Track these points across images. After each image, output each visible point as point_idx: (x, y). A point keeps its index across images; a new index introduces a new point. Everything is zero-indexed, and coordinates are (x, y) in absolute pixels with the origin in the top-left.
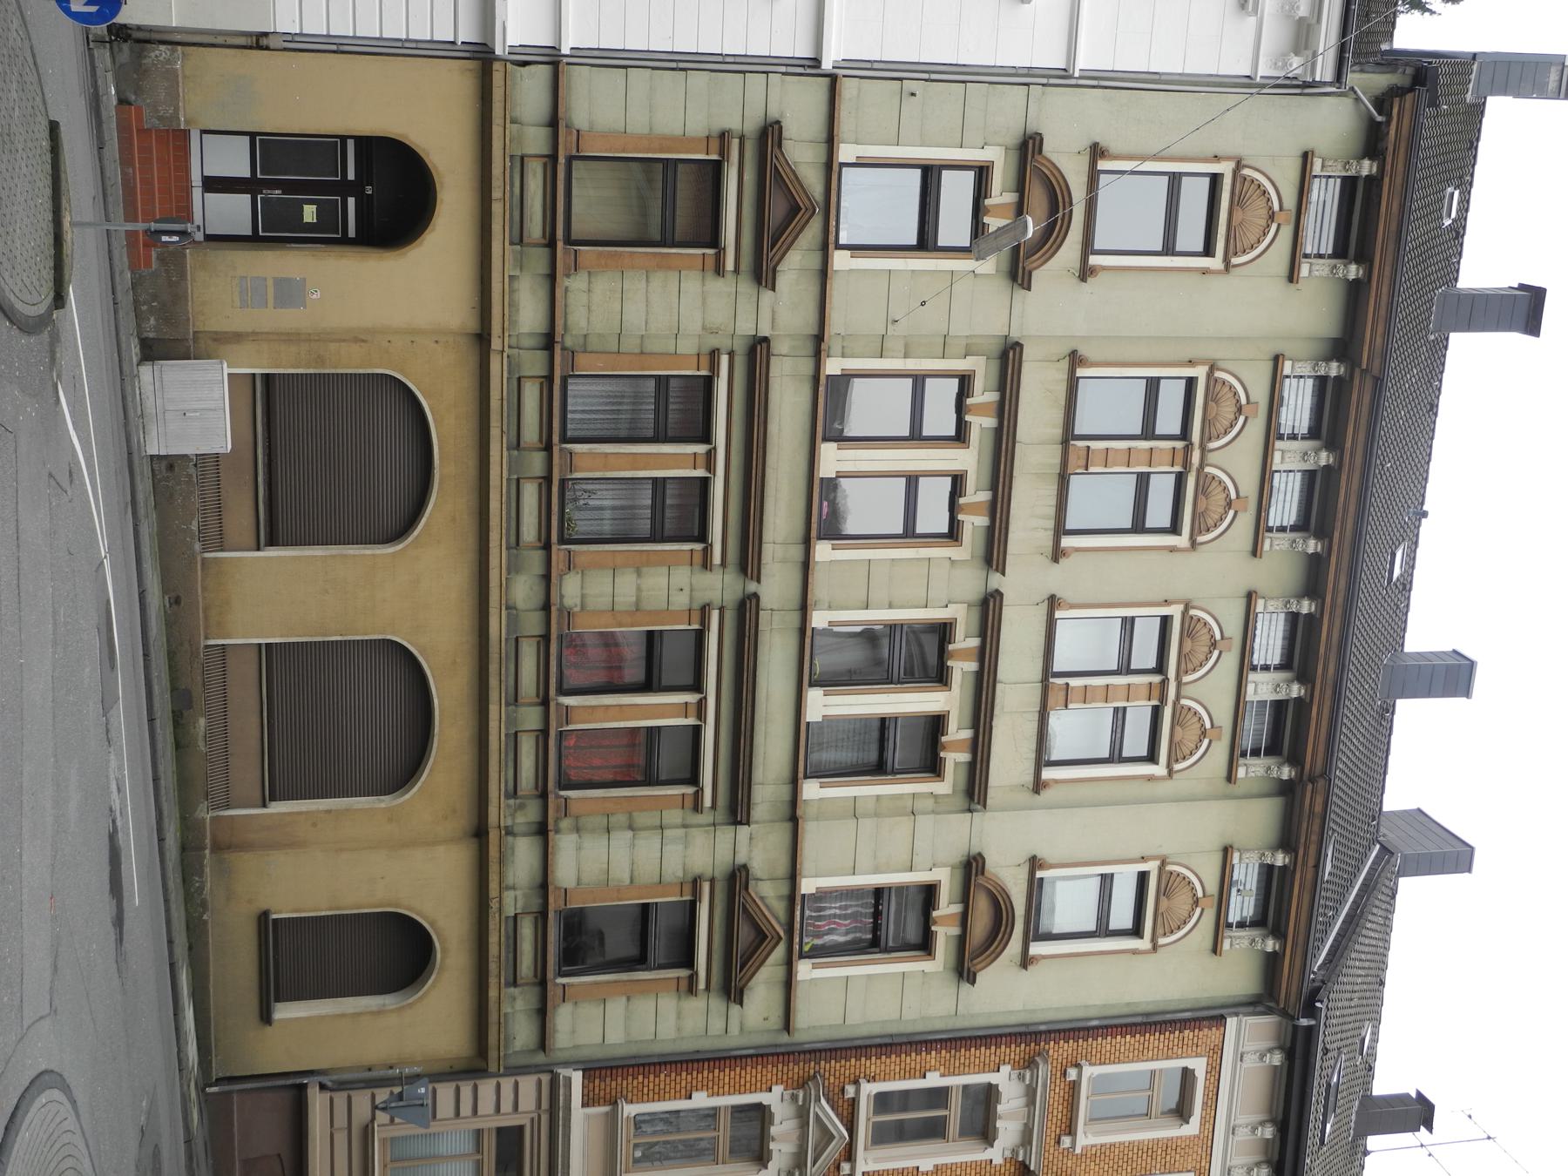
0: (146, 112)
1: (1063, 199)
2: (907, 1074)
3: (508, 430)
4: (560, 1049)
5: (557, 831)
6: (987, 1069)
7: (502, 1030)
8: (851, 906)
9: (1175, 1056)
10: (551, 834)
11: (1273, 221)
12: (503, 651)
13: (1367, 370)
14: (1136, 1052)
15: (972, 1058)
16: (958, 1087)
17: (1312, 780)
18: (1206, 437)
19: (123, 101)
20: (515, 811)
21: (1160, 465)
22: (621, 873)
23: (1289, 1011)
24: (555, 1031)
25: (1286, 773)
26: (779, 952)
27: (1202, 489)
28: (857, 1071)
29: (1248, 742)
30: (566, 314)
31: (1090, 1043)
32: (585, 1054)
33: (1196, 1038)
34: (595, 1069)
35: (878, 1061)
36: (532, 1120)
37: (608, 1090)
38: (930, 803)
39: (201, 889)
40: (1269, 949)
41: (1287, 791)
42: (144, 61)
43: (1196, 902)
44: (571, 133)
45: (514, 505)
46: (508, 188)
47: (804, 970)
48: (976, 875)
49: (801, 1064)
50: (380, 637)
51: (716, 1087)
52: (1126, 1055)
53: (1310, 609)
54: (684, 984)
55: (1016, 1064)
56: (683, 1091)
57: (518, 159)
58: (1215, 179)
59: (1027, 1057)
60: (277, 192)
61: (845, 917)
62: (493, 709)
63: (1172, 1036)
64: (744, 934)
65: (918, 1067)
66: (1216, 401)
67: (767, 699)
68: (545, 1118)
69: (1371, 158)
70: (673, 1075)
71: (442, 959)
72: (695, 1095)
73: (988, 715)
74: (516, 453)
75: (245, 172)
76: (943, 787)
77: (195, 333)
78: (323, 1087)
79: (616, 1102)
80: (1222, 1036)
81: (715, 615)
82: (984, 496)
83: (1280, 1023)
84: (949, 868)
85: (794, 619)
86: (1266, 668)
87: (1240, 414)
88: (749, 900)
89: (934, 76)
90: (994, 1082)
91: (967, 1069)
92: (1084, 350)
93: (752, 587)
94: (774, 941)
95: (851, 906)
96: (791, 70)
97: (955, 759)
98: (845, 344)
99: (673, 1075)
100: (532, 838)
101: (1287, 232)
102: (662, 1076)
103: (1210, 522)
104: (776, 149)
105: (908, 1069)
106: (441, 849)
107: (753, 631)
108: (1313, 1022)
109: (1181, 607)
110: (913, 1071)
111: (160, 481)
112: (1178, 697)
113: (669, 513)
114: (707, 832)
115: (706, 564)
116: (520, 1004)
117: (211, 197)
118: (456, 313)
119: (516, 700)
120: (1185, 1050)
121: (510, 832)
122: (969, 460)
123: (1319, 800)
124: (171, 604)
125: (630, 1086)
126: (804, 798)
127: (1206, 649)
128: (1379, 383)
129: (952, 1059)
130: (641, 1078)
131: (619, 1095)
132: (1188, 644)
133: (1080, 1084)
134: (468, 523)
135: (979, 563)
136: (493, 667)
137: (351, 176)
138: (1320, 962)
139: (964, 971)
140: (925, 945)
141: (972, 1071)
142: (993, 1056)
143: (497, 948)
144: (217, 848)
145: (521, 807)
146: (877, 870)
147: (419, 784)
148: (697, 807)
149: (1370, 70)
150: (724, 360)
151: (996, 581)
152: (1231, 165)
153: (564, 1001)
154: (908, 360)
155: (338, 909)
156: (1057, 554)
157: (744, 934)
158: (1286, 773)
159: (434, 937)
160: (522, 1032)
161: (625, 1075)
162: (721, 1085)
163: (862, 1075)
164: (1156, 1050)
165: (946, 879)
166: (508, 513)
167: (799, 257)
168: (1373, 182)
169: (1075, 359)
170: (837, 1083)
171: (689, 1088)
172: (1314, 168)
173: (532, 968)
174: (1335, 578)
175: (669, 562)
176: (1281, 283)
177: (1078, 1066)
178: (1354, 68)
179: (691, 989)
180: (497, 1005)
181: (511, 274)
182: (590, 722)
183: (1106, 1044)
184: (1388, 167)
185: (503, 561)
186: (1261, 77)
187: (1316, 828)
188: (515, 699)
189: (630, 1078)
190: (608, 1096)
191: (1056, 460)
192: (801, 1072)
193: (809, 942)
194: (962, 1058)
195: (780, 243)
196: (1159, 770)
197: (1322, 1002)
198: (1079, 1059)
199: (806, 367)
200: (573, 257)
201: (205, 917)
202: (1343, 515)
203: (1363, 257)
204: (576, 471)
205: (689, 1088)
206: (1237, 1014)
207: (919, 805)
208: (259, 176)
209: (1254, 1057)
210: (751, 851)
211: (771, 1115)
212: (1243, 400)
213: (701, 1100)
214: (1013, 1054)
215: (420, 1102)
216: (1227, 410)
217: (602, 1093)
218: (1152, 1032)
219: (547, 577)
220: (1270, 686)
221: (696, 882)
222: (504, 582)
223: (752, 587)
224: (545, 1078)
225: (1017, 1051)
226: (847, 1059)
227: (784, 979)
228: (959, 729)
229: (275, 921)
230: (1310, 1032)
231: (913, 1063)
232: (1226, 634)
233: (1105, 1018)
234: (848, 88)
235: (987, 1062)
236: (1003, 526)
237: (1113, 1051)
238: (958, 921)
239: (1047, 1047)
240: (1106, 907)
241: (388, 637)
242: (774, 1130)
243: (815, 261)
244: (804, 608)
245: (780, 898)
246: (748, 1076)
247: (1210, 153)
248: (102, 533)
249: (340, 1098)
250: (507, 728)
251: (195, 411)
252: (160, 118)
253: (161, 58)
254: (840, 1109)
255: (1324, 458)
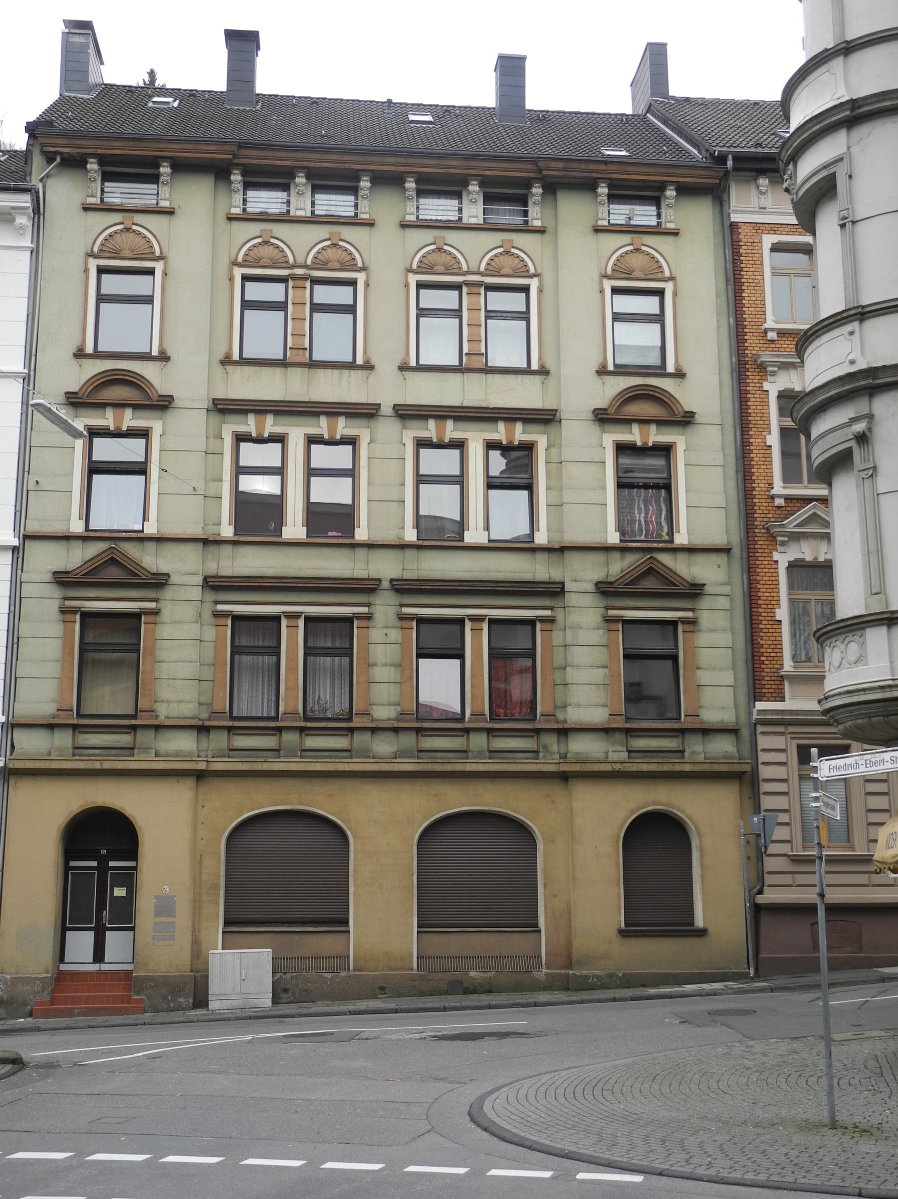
0: (39, 999)
1: (110, 376)
2: (768, 459)
3: (263, 757)
4: (737, 718)
5: (565, 721)
6: (766, 400)
7: (716, 761)
8: (639, 505)
9: (760, 259)
10: (566, 726)
11: (130, 229)
12: (425, 761)
13: (233, 154)
14: (756, 288)
15: (756, 411)
16: (780, 421)
17: (540, 171)
18: (286, 265)
19: (31, 1014)
20: (549, 752)
21: (304, 296)
22: (599, 675)
23: (722, 175)
24: (722, 722)
25: (537, 190)
26: (666, 559)
27: (323, 265)
28: (763, 497)
29: (518, 220)
30: (184, 718)
31: (748, 323)
32: (742, 699)
33: (747, 244)
34: (755, 692)
35: (756, 481)
36: (792, 738)
37: (772, 682)
38: (554, 451)
39: (598, 977)
40: (674, 193)
41: (551, 189)
42: (5, 999)
43: (637, 250)
44: (58, 715)
45: (321, 753)
46: (93, 758)
47: (681, 539)
48: (608, 414)
49: (756, 539)
50: (415, 848)
51: (773, 602)
52: (759, 295)
53: (476, 185)
54: (689, 627)
55: (763, 378)
56: (775, 626)
57: (76, 751)
58: (101, 271)
59: (757, 370)
60: (104, 914)
61: (647, 510)
62: (469, 768)
63: (744, 262)
64: (114, 573)
65: (763, 451)
66: (259, 260)
67: (471, 571)
68: (792, 729)
69: (86, 162)
70: (761, 634)
71: (661, 804)
72: (778, 618)
73: (485, 411)
74: (282, 752)
75: (91, 935)
76: (542, 442)
77: (191, 972)
78: (760, 892)
79: (782, 676)
80: (746, 224)
81: (406, 610)
82: (323, 421)
83: (737, 181)
84: (604, 435)
85: (410, 554)
86: (460, 210)
87: (269, 242)
88: (621, 581)
89: (26, 469)
90: (776, 394)
91: (765, 415)
92: (221, 355)
93: (386, 584)
94: (654, 562)
95: (639, 505)
96: (20, 566)
97: (520, 434)
98: (211, 523)
99: (761, 634)
100: (569, 740)
101: (139, 218)
102: (762, 642)
103: (348, 258)
104: (70, 575)
105: (764, 459)
106: (574, 805)
107: (416, 583)
108: (730, 157)
109: (410, 275)
110: (765, 455)
111: (295, 998)
112: (478, 273)
113: (338, 645)
114: (569, 614)
115: (368, 617)
116: (698, 748)
117: (107, 958)
118: (183, 791)
119: (465, 751)
120: (756, 252)
121: (564, 756)
122: (296, 434)
123: (554, 164)
124: (385, 994)
125: (769, 666)
126: (547, 543)
127: (443, 255)
128: (241, 145)
129: (757, 426)
130: (762, 658)
131: (776, 674)
132: (438, 268)
133: (780, 329)
134: (333, 786)
135: (373, 422)
136: (438, 768)
137: (94, 864)
138: (696, 152)
139: (686, 420)
140: (666, 450)
141: (767, 411)
142: (755, 396)
143: (651, 764)
144: (569, 965)
145: (545, 747)
146: (604, 488)
147: (527, 821)
148: (551, 620)
149: (29, 169)
150: (220, 607)
151: (386, 409)
152: (91, 260)
153: (698, 716)
154: (224, 479)
155: (619, 879)
156: (368, 366)
157: (649, 584)
158: (537, 190)
159: (644, 810)
160: (723, 746)
161: (760, 670)
162: (771, 598)
163: (767, 493)
164: (755, 273)
165: (611, 437)
166: (326, 757)
167: (148, 557)
168: (103, 161)
169: (227, 361)
170: (773, 512)
171: (772, 622)
172: (93, 202)
173: (670, 739)
174: (388, 165)
175: (366, 644)
176: (175, 219)
177: (766, 331)
178: (28, 180)
179: (693, 622)
180: (696, 765)
181: (154, 755)
182: (483, 698)
183: (749, 312)
184: (91, 151)
185: (411, 761)
186: (32, 243)
187: (575, 165)
188: (464, 752)
189: (763, 666)
190: (777, 682)
191: (298, 371)
192: (763, 539)
193: (667, 538)
194: (756, 418)
195: (136, 571)
196: (534, 284)
197: (715, 151)
198: (761, 331)
199: (227, 550)
200: (144, 713)
201: (620, 975)
202: (340, 163)
203: (155, 163)
204: (297, 710)
205: (772, 622)
206: (729, 214)
207: (554, 458)
208: (93, 926)
209: (763, 199)
210: (585, 581)
211: (796, 560)
212: (259, 240)
213: (783, 613)
214: (754, 381)
215: (762, 821)
216: (266, 251)
217: (774, 687)
218: (741, 277)
219: (374, 730)
220: (472, 206)
221: (608, 620)
222: (375, 760)
223: (386, 584)
224: (760, 729)
225: (752, 378)
226: (754, 504)
227: (687, 554)
228: (497, 432)
229: (626, 925)
230: (738, 158)
231: (759, 455)
232: (432, 241)
233: (729, 312)
234: (33, 527)
235: (760, 400)
236: (343, 406)
237: (755, 306)
238: (645, 427)
239: (749, 355)
240: (642, 317)
241: (415, 842)
242: (809, 558)
243: (151, 546)
244: (403, 547)
245: (622, 558)
246: (765, 578)
247: (82, 276)
248: (210, 1041)
249: (769, 879)
250: (485, 758)
251: (241, 973)
252: (43, 989)
253: (3, 988)
254: (794, 509)
255: (301, 179)
